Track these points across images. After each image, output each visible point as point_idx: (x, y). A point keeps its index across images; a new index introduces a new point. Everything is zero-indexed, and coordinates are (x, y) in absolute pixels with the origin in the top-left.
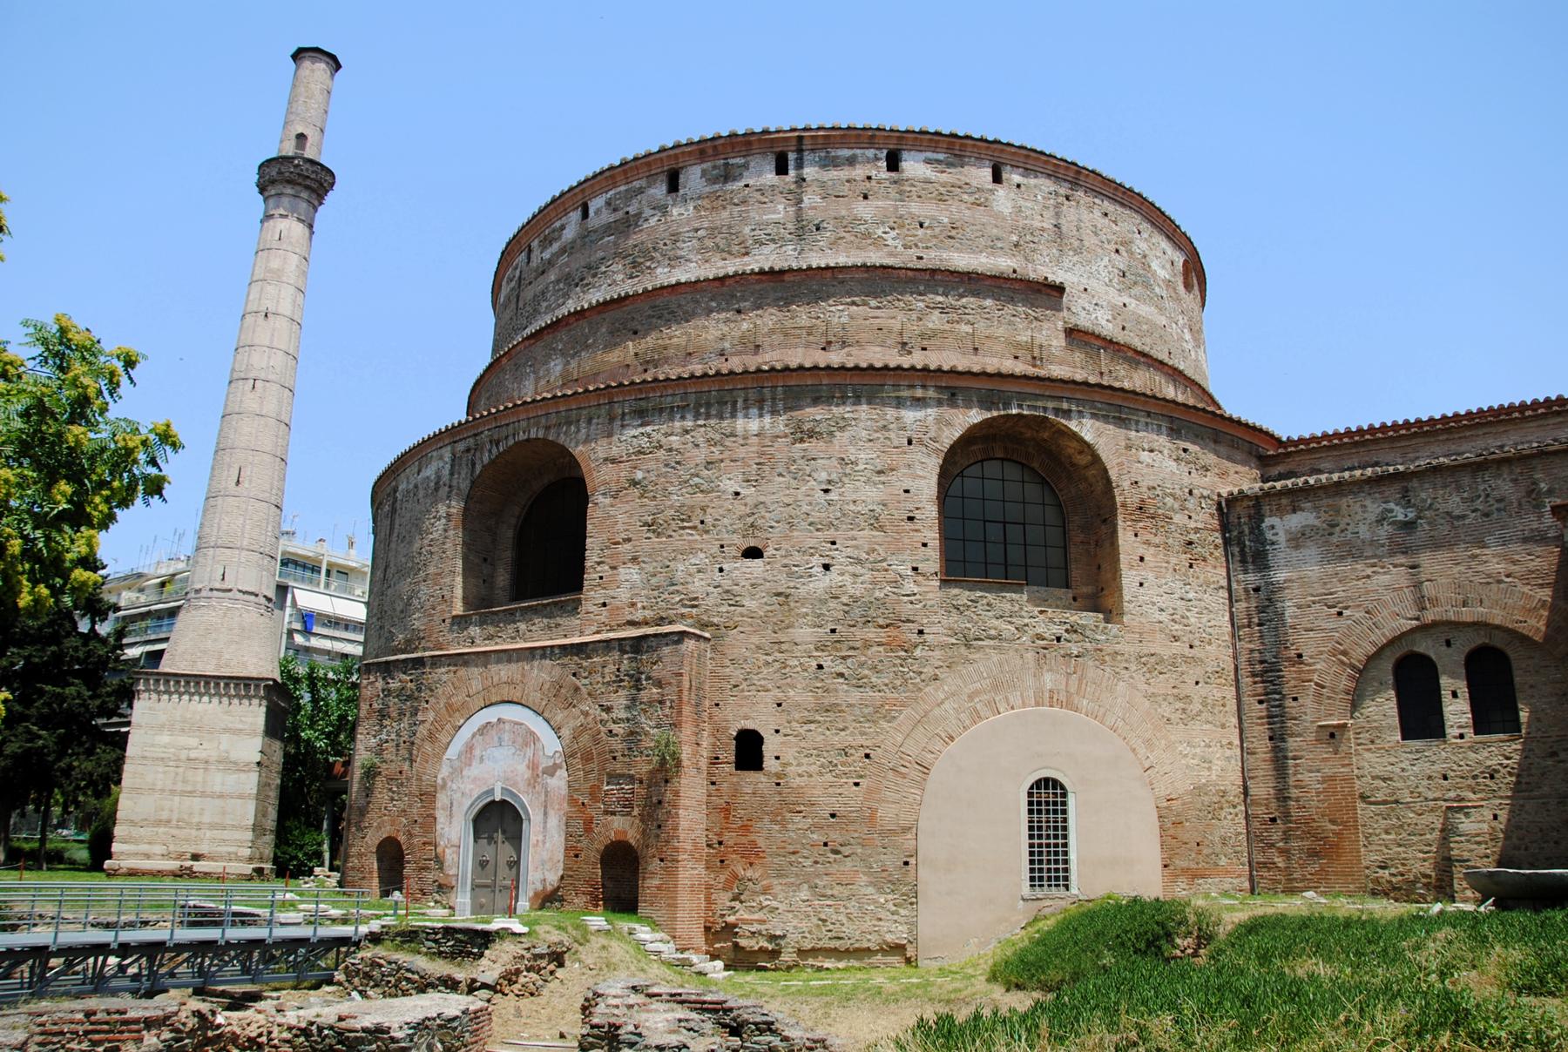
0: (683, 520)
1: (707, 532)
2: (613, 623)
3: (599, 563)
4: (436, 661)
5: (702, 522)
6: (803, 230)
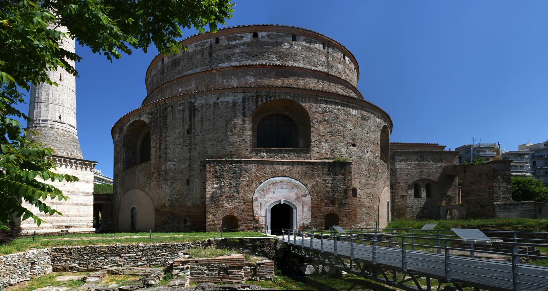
0: (338, 133)
1: (345, 138)
2: (321, 158)
3: (315, 141)
4: (247, 162)
5: (343, 135)
6: (329, 66)
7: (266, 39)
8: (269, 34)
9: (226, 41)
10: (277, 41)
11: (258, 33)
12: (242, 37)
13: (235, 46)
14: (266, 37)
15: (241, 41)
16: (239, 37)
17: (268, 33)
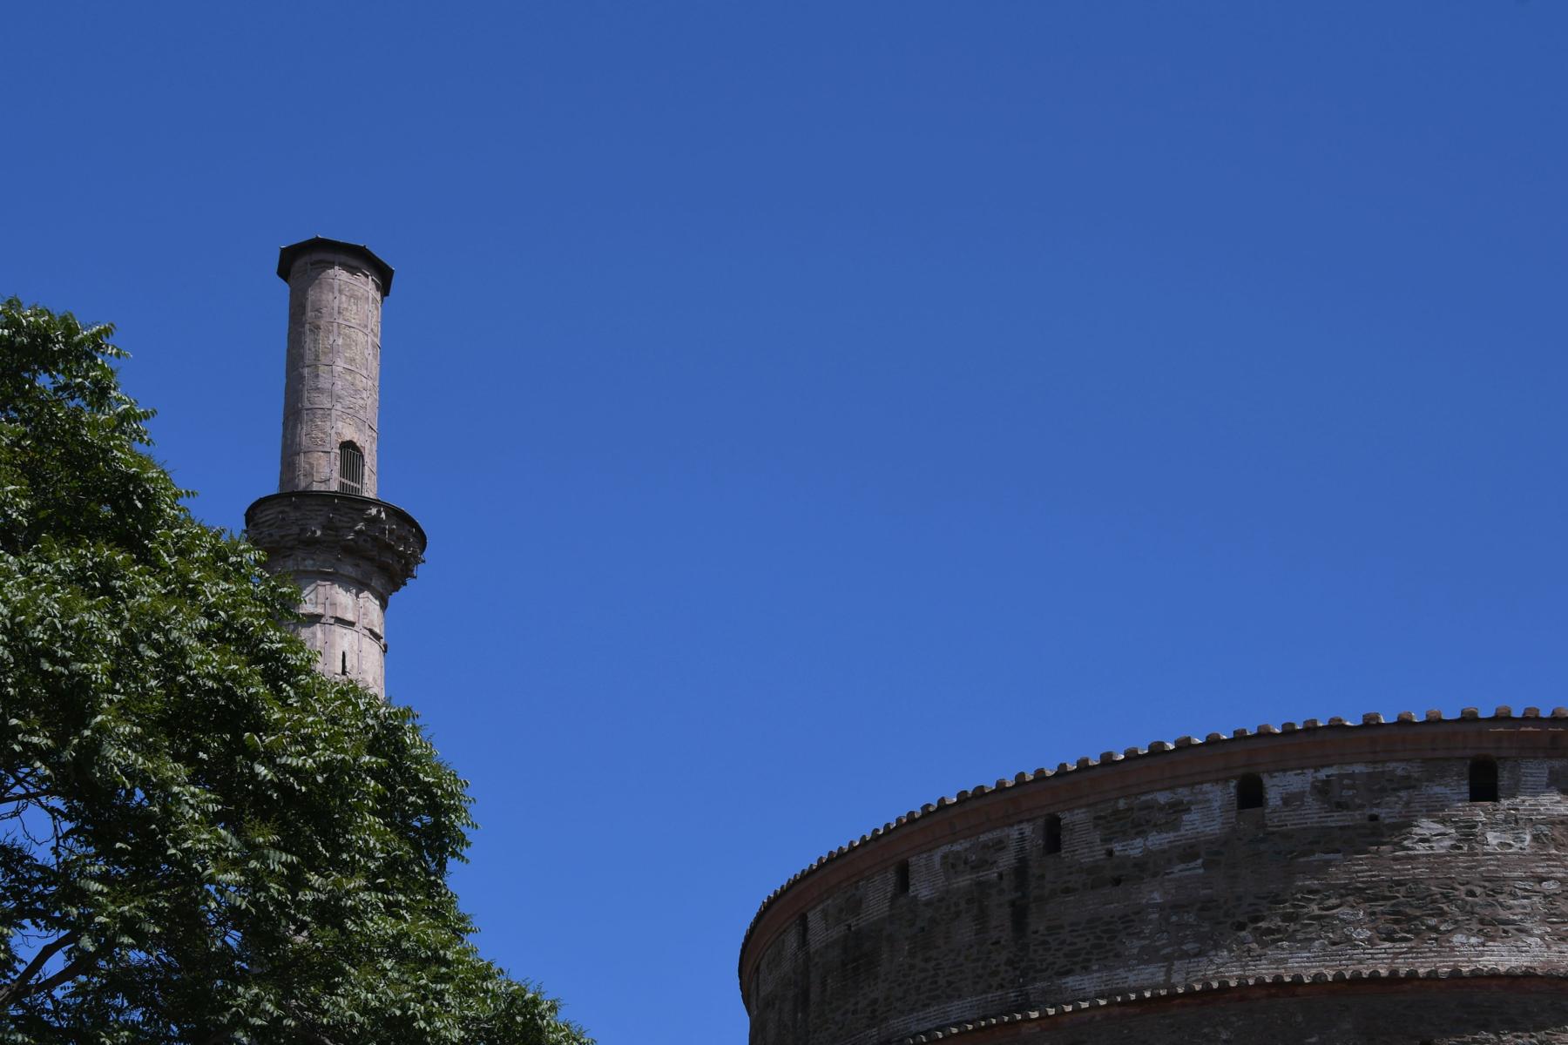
7: (1313, 814)
8: (1327, 781)
9: (1096, 837)
10: (1374, 818)
11: (1267, 781)
12: (1179, 808)
13: (1144, 868)
14: (1309, 799)
15: (1171, 836)
16: (1161, 808)
17: (1322, 774)
